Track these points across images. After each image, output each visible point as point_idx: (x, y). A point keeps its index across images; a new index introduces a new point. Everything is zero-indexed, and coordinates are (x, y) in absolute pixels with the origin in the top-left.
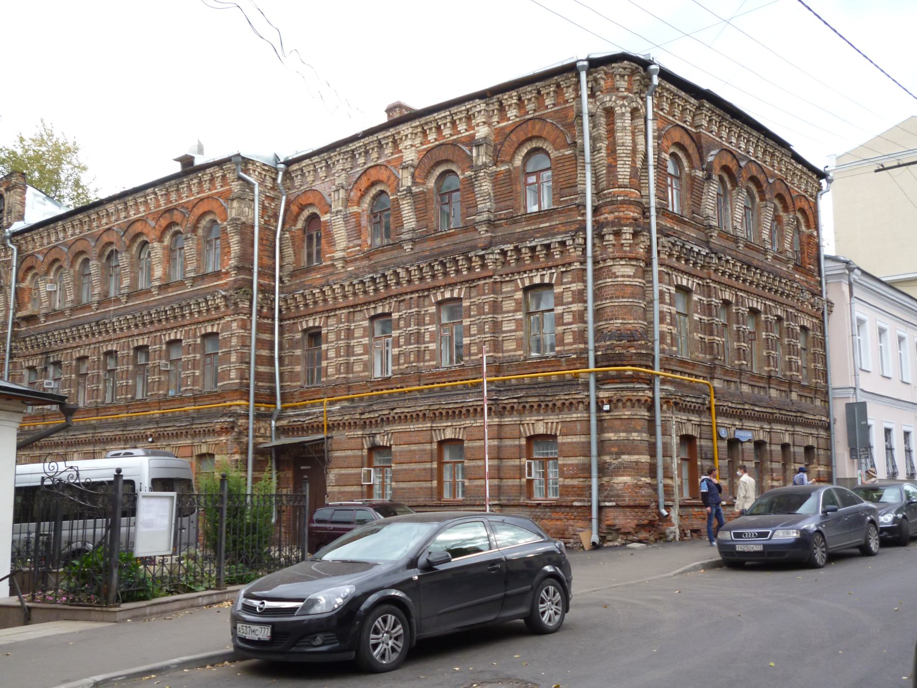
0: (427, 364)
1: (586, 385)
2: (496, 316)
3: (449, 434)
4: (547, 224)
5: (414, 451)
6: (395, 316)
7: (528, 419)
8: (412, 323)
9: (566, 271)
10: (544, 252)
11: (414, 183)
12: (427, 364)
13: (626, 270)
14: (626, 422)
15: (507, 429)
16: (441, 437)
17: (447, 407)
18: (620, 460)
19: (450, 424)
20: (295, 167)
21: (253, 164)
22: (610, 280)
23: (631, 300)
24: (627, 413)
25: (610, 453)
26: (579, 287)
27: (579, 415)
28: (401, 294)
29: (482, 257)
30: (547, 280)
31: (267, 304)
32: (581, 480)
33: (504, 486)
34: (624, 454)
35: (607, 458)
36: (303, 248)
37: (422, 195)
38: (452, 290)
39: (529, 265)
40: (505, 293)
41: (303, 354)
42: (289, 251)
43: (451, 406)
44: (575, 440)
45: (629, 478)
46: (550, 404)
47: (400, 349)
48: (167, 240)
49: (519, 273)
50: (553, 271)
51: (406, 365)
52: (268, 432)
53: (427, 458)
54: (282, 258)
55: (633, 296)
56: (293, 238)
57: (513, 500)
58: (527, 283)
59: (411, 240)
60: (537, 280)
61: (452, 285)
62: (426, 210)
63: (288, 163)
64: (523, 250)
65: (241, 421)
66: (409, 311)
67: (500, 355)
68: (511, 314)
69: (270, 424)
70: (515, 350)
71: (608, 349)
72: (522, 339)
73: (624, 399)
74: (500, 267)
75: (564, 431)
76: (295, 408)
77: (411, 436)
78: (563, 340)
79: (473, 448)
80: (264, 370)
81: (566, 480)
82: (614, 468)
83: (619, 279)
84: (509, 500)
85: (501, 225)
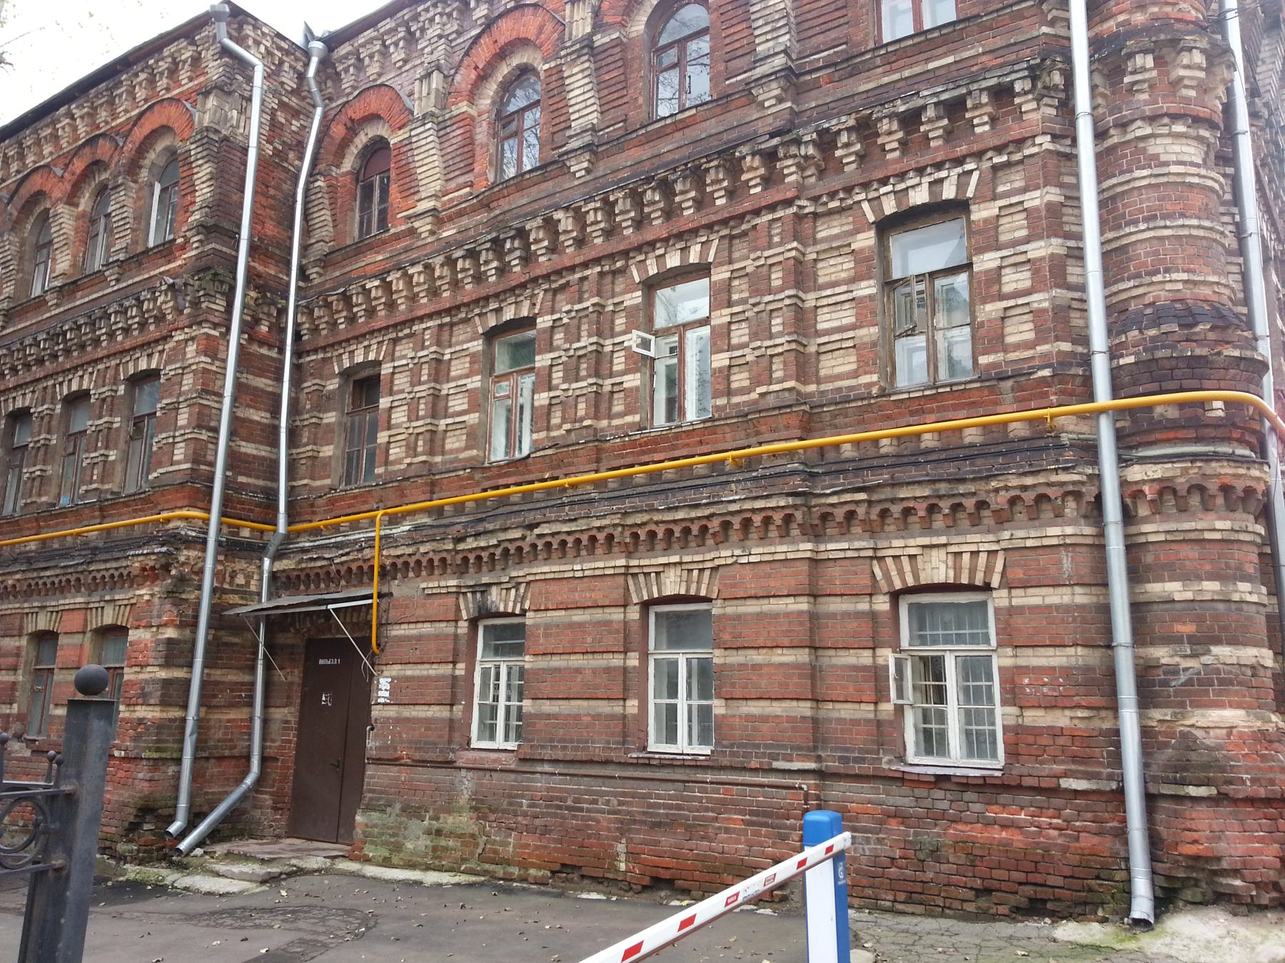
0: (615, 422)
1: (1090, 451)
2: (801, 294)
3: (672, 584)
4: (950, 59)
5: (581, 625)
6: (544, 322)
8: (584, 334)
9: (1008, 165)
10: (945, 122)
11: (598, 26)
12: (615, 422)
13: (1185, 149)
14: (1215, 550)
15: (835, 571)
16: (650, 592)
17: (669, 517)
18: (1206, 659)
19: (675, 559)
20: (345, 49)
22: (1145, 172)
23: (1207, 223)
24: (1220, 524)
25: (1171, 640)
26: (1049, 198)
27: (1069, 530)
28: (559, 273)
29: (770, 157)
30: (949, 192)
31: (269, 315)
32: (1080, 713)
33: (830, 720)
34: (1217, 641)
35: (1162, 654)
36: (352, 210)
37: (618, 49)
39: (896, 161)
40: (825, 240)
41: (340, 423)
42: (323, 216)
43: (680, 515)
45: (1241, 713)
47: (552, 394)
48: (85, 202)
49: (866, 186)
50: (970, 166)
51: (567, 426)
53: (610, 641)
54: (307, 231)
55: (1207, 213)
56: (332, 189)
57: (857, 760)
58: (890, 207)
59: (587, 147)
60: (920, 197)
61: (683, 236)
62: (625, 84)
63: (333, 41)
64: (885, 126)
65: (185, 554)
66: (577, 307)
67: (812, 388)
68: (844, 288)
69: (260, 567)
70: (855, 374)
71: (1156, 348)
72: (874, 344)
73: (1213, 486)
74: (813, 180)
75: (1017, 573)
76: (316, 532)
77: (574, 590)
78: (1003, 336)
79: (738, 617)
80: (255, 452)
81: (1027, 713)
82: (1189, 682)
83: (1174, 169)
84: (844, 760)
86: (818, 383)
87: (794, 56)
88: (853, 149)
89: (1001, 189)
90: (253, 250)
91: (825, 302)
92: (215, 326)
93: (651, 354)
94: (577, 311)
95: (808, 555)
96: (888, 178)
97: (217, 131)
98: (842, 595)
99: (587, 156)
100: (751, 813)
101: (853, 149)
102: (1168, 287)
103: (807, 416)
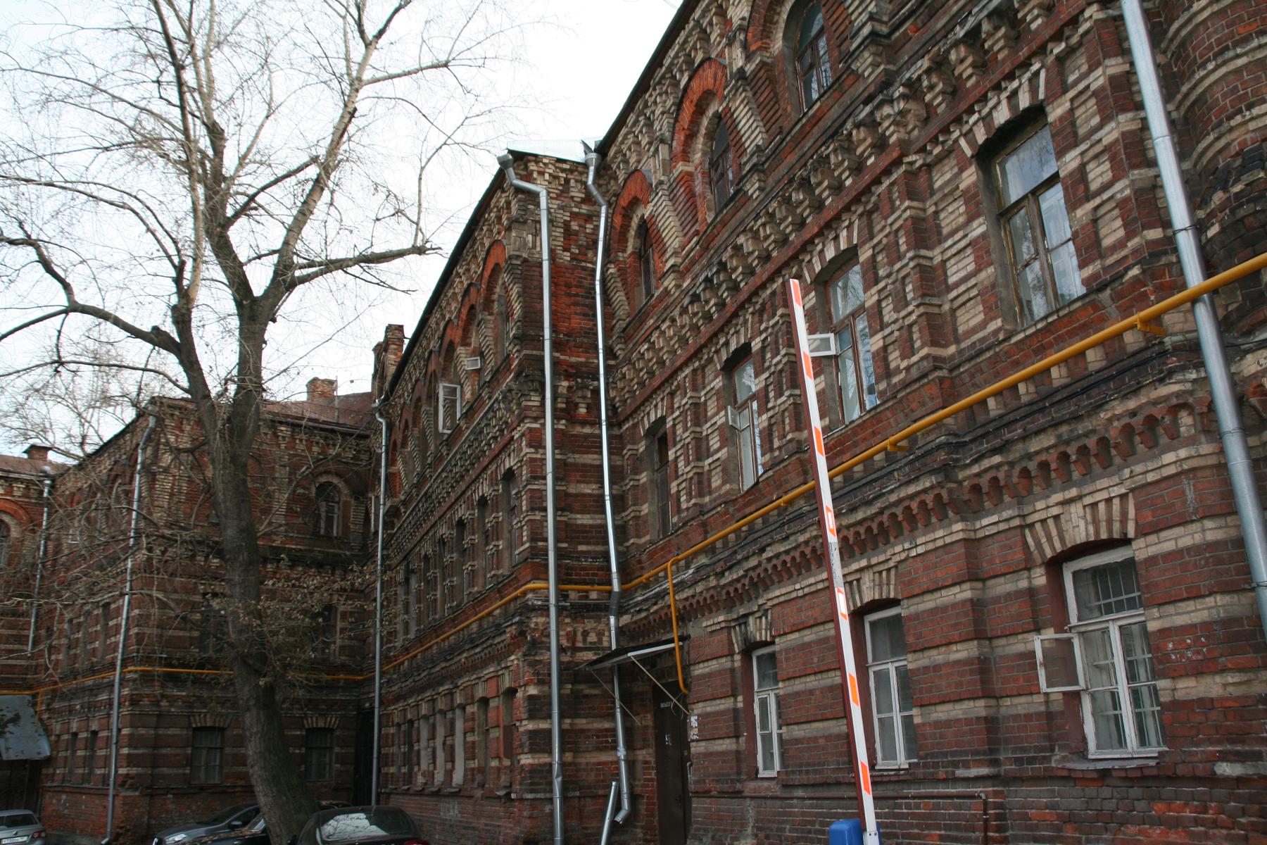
1: (1192, 351)
2: (923, 252)
5: (808, 645)
7: (1044, 506)
9: (1070, 51)
10: (1003, 30)
11: (748, 58)
15: (993, 548)
19: (864, 563)
21: (537, 162)
27: (1183, 453)
30: (1024, 101)
31: (584, 397)
36: (638, 285)
38: (836, 238)
39: (976, 85)
41: (651, 481)
42: (619, 297)
44: (1186, 542)
46: (1091, 442)
52: (605, 639)
57: (1031, 761)
60: (1002, 115)
61: (830, 226)
62: (776, 98)
63: (603, 148)
67: (952, 349)
68: (961, 234)
69: (608, 624)
74: (916, 132)
75: (1149, 517)
77: (800, 610)
79: (917, 616)
80: (591, 522)
84: (1018, 761)
85: (906, 38)
86: (957, 341)
87: (885, 19)
88: (937, 89)
89: (1071, 79)
90: (556, 345)
91: (949, 253)
92: (536, 419)
93: (832, 352)
94: (773, 326)
95: (961, 536)
96: (972, 106)
97: (518, 257)
98: (1004, 575)
99: (756, 177)
100: (947, 827)
101: (937, 89)
102: (1252, 126)
103: (946, 385)
